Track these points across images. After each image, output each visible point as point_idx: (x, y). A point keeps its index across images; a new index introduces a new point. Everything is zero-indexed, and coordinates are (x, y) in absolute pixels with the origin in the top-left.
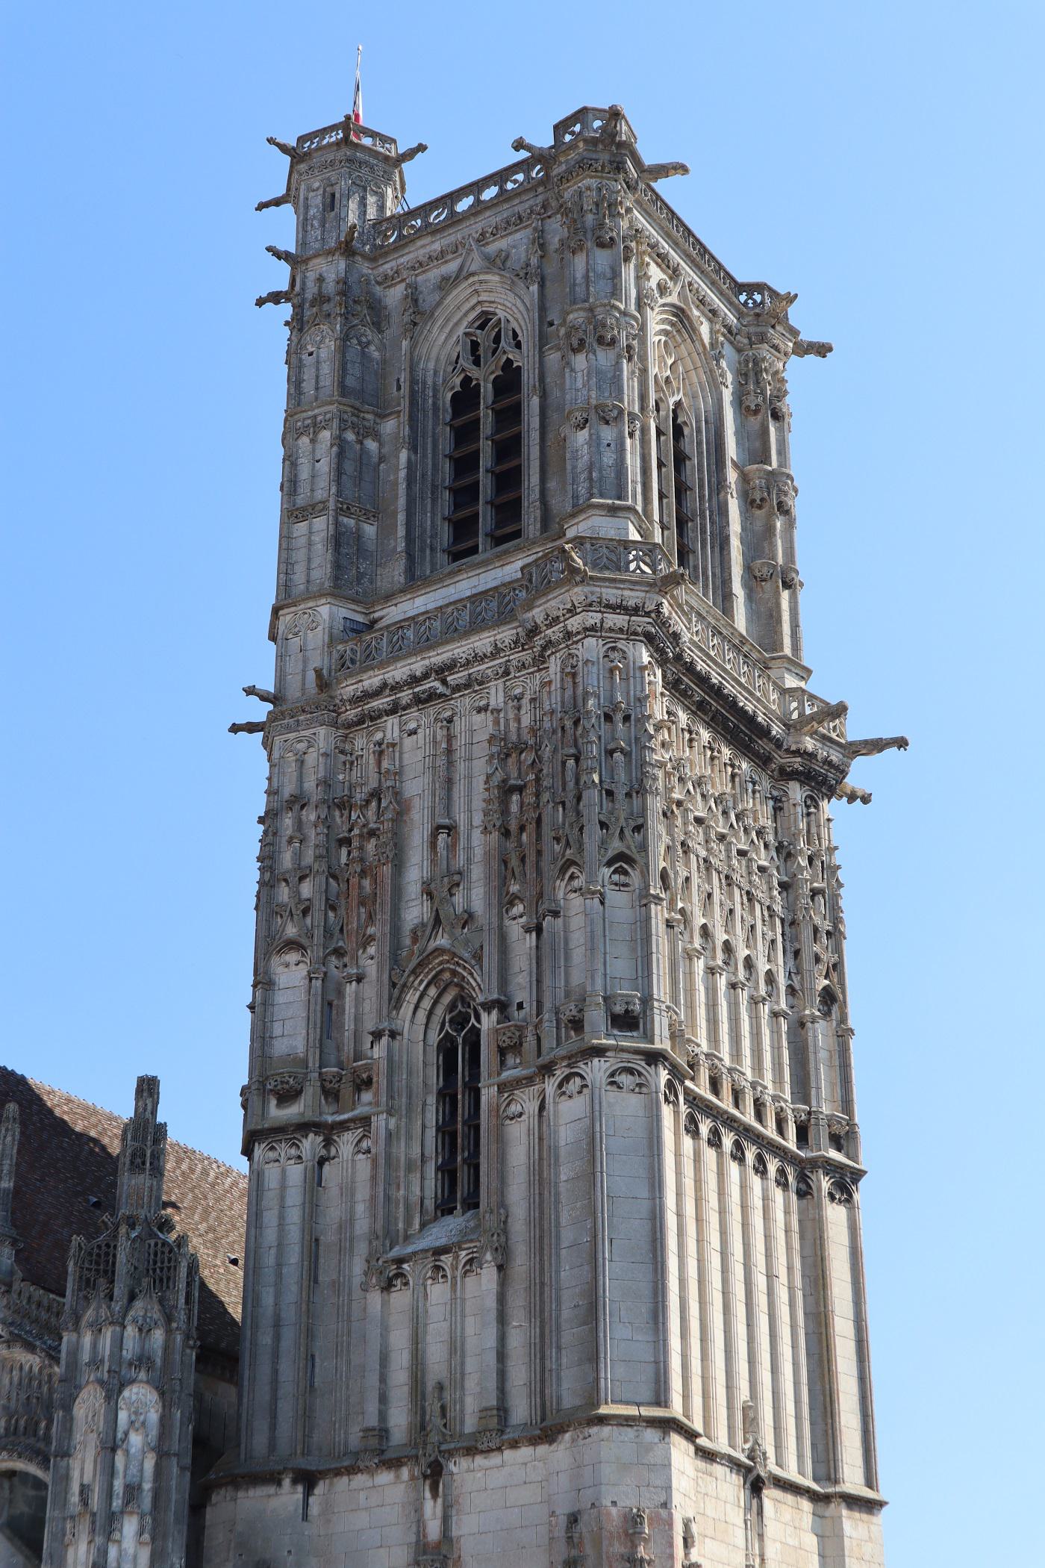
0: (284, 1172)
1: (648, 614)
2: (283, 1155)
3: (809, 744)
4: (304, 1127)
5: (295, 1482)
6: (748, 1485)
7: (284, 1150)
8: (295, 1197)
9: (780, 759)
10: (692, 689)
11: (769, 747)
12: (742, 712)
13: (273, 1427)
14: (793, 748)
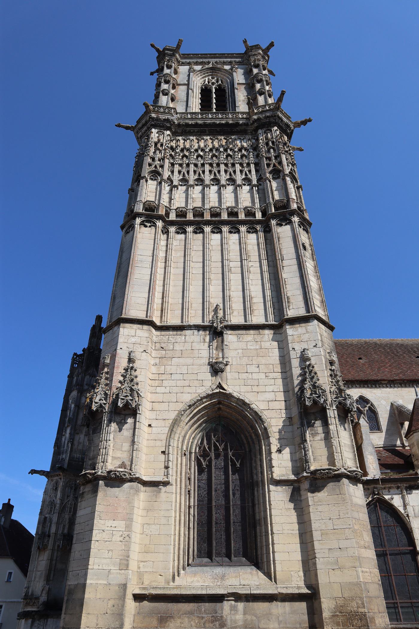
1: (149, 121)
3: (255, 117)
6: (211, 332)
9: (250, 128)
10: (192, 130)
11: (243, 128)
12: (220, 125)
14: (252, 122)
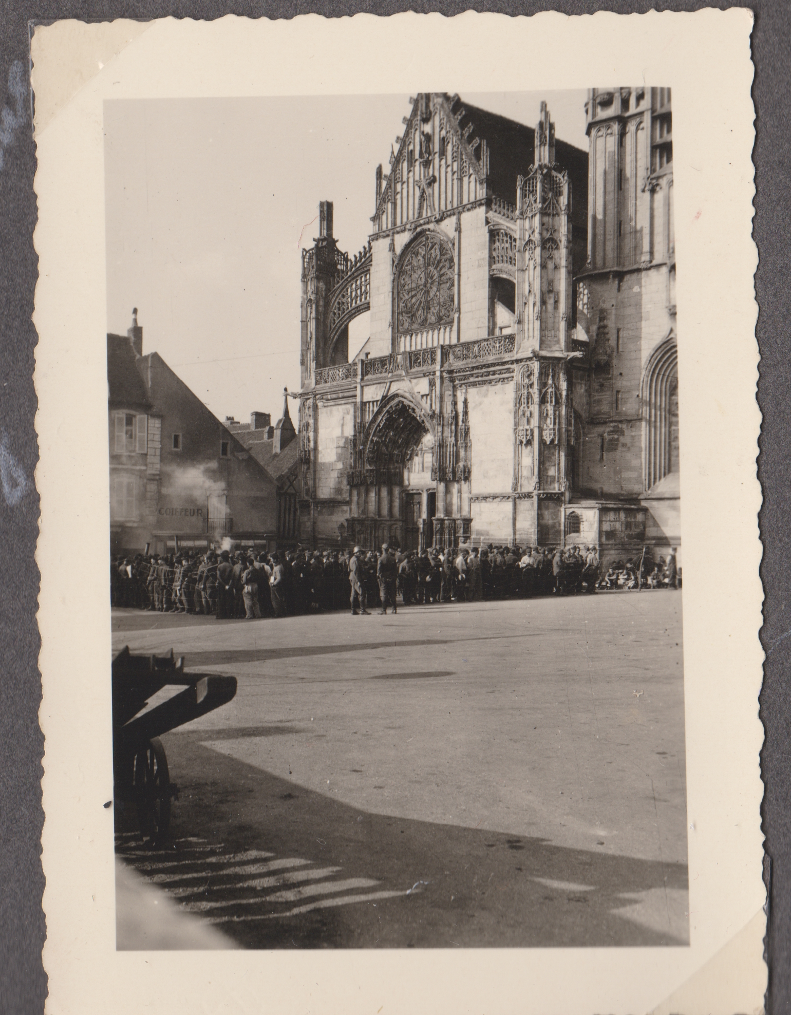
5: (614, 277)
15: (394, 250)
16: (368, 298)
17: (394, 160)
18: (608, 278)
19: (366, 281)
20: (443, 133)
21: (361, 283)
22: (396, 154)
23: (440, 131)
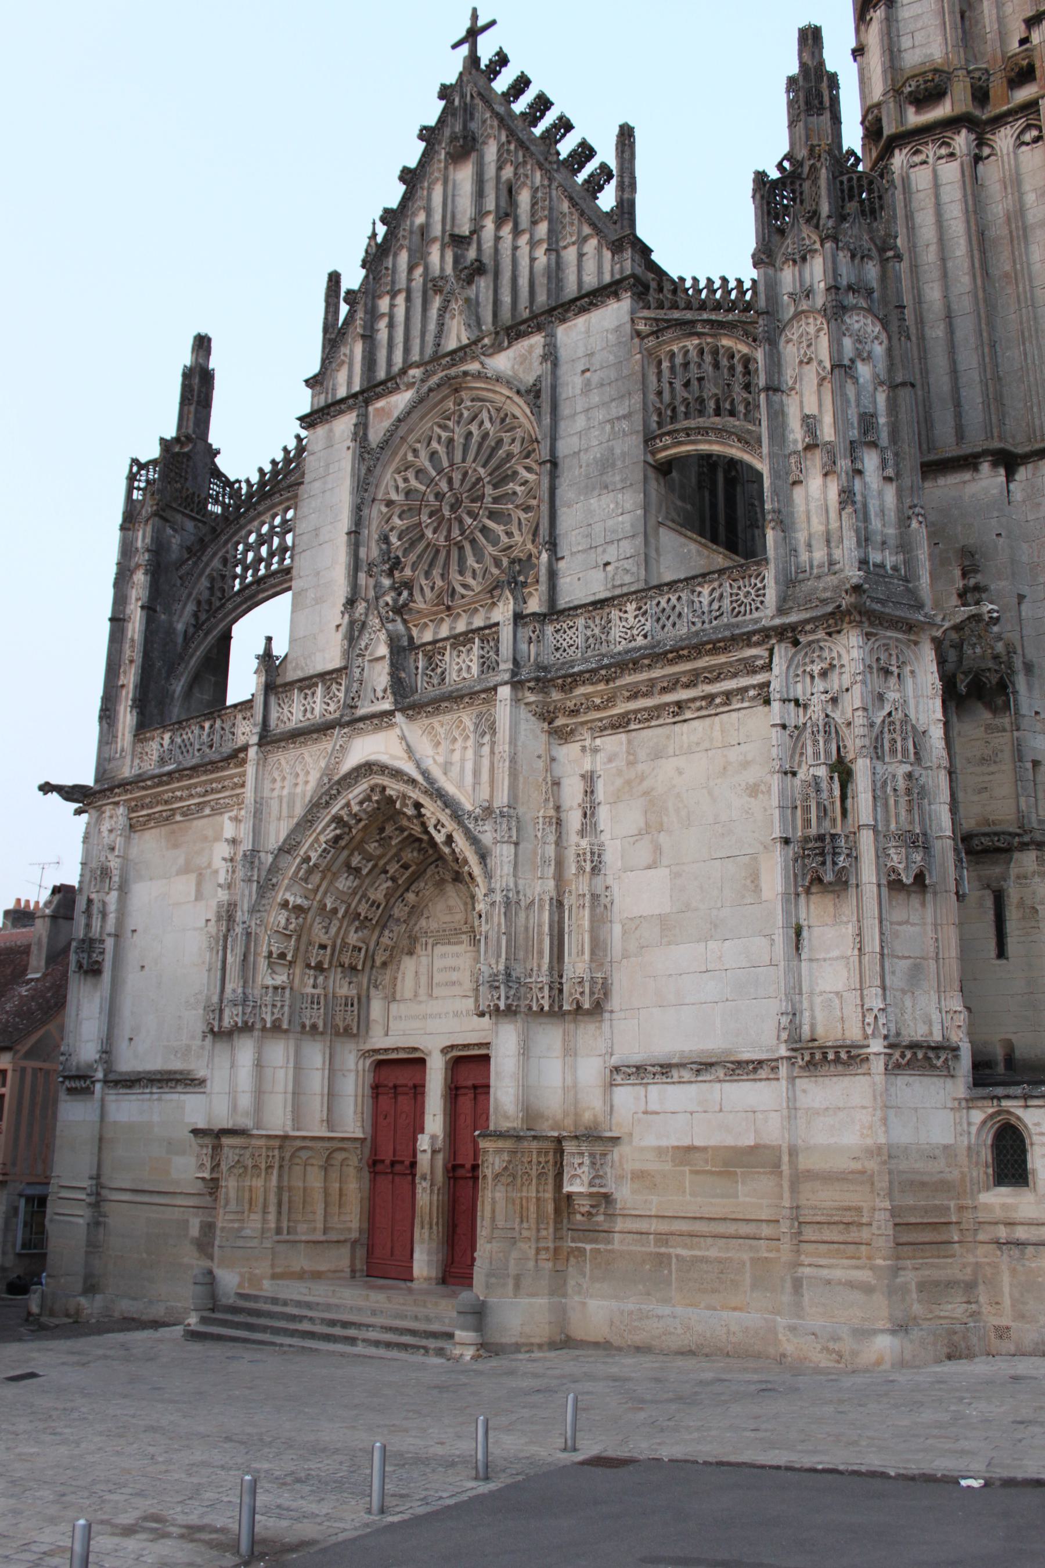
0: (935, 173)
2: (931, 155)
4: (953, 123)
5: (995, 465)
7: (930, 151)
8: (953, 194)
13: (958, 415)
15: (365, 434)
16: (287, 562)
17: (374, 250)
18: (975, 468)
19: (284, 522)
20: (508, 172)
21: (272, 527)
22: (379, 239)
23: (500, 169)
